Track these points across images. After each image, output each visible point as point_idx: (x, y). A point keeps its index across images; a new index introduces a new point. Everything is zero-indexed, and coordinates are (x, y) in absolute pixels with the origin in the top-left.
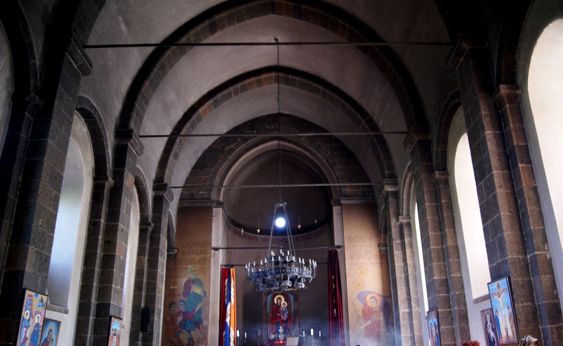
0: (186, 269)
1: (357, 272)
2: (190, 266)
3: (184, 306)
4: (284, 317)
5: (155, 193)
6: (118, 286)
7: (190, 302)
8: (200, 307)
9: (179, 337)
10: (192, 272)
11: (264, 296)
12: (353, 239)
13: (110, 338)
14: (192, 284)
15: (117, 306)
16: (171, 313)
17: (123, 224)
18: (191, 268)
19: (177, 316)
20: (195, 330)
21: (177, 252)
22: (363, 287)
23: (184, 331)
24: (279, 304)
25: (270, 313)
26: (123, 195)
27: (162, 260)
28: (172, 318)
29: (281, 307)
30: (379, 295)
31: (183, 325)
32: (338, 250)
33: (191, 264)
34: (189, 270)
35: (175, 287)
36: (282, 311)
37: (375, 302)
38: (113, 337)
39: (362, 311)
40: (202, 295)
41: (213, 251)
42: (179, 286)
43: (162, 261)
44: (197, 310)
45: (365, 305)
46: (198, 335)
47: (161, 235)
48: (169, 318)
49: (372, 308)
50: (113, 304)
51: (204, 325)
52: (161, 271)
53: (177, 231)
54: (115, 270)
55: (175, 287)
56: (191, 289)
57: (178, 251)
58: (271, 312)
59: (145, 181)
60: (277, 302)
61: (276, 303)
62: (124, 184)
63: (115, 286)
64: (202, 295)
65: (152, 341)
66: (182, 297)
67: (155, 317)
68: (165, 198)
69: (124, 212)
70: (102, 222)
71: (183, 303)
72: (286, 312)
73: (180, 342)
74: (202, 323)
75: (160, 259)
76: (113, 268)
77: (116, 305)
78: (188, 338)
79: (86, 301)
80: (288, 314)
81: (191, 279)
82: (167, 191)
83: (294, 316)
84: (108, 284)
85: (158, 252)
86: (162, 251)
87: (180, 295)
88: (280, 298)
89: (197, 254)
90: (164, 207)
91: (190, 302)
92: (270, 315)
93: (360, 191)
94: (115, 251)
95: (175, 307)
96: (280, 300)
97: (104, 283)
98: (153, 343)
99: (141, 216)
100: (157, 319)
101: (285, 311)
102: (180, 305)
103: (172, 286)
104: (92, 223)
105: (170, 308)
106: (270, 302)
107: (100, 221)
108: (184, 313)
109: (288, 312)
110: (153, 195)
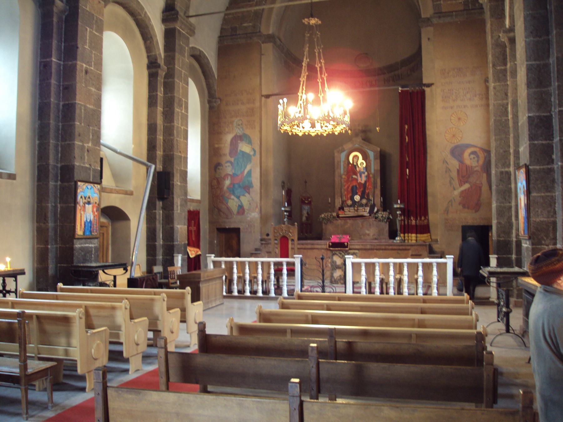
0: (232, 123)
1: (452, 118)
3: (231, 167)
4: (362, 180)
5: (165, 26)
6: (88, 143)
9: (227, 203)
10: (239, 127)
12: (448, 73)
13: (79, 207)
14: (239, 141)
15: (90, 169)
16: (217, 176)
17: (89, 63)
19: (224, 179)
20: (245, 196)
21: (219, 102)
22: (459, 139)
23: (233, 197)
24: (355, 164)
25: (344, 174)
26: (80, 23)
27: (183, 111)
28: (219, 183)
29: (358, 167)
30: (481, 149)
31: (232, 189)
32: (427, 90)
33: (237, 117)
34: (235, 124)
37: (476, 159)
38: (84, 207)
39: (456, 171)
40: (252, 153)
41: (263, 99)
43: (182, 113)
44: (246, 172)
45: (461, 162)
47: (176, 80)
48: (215, 182)
49: (471, 166)
50: (79, 166)
52: (182, 125)
53: (218, 76)
54: (77, 123)
56: (238, 147)
57: (220, 102)
58: (346, 173)
59: (142, 9)
61: (351, 162)
62: (80, 8)
63: (81, 144)
64: (252, 153)
65: (173, 210)
66: (228, 158)
67: (175, 180)
68: (179, 31)
69: (87, 47)
70: (54, 61)
72: (364, 173)
73: (228, 208)
75: (177, 110)
76: (74, 120)
77: (86, 167)
78: (237, 205)
79: (44, 164)
80: (366, 176)
82: (179, 22)
83: (374, 178)
84: (70, 141)
85: (174, 101)
86: (180, 100)
87: (226, 154)
88: (356, 156)
89: (243, 103)
90: (180, 45)
92: (344, 177)
93: (461, 2)
94: (75, 98)
95: (222, 169)
97: (66, 141)
98: (175, 212)
99: (148, 57)
100: (179, 184)
102: (226, 167)
103: (217, 144)
104: (43, 63)
105: (215, 170)
106: (344, 162)
107: (52, 61)
108: (233, 176)
109: (366, 173)
110: (164, 29)
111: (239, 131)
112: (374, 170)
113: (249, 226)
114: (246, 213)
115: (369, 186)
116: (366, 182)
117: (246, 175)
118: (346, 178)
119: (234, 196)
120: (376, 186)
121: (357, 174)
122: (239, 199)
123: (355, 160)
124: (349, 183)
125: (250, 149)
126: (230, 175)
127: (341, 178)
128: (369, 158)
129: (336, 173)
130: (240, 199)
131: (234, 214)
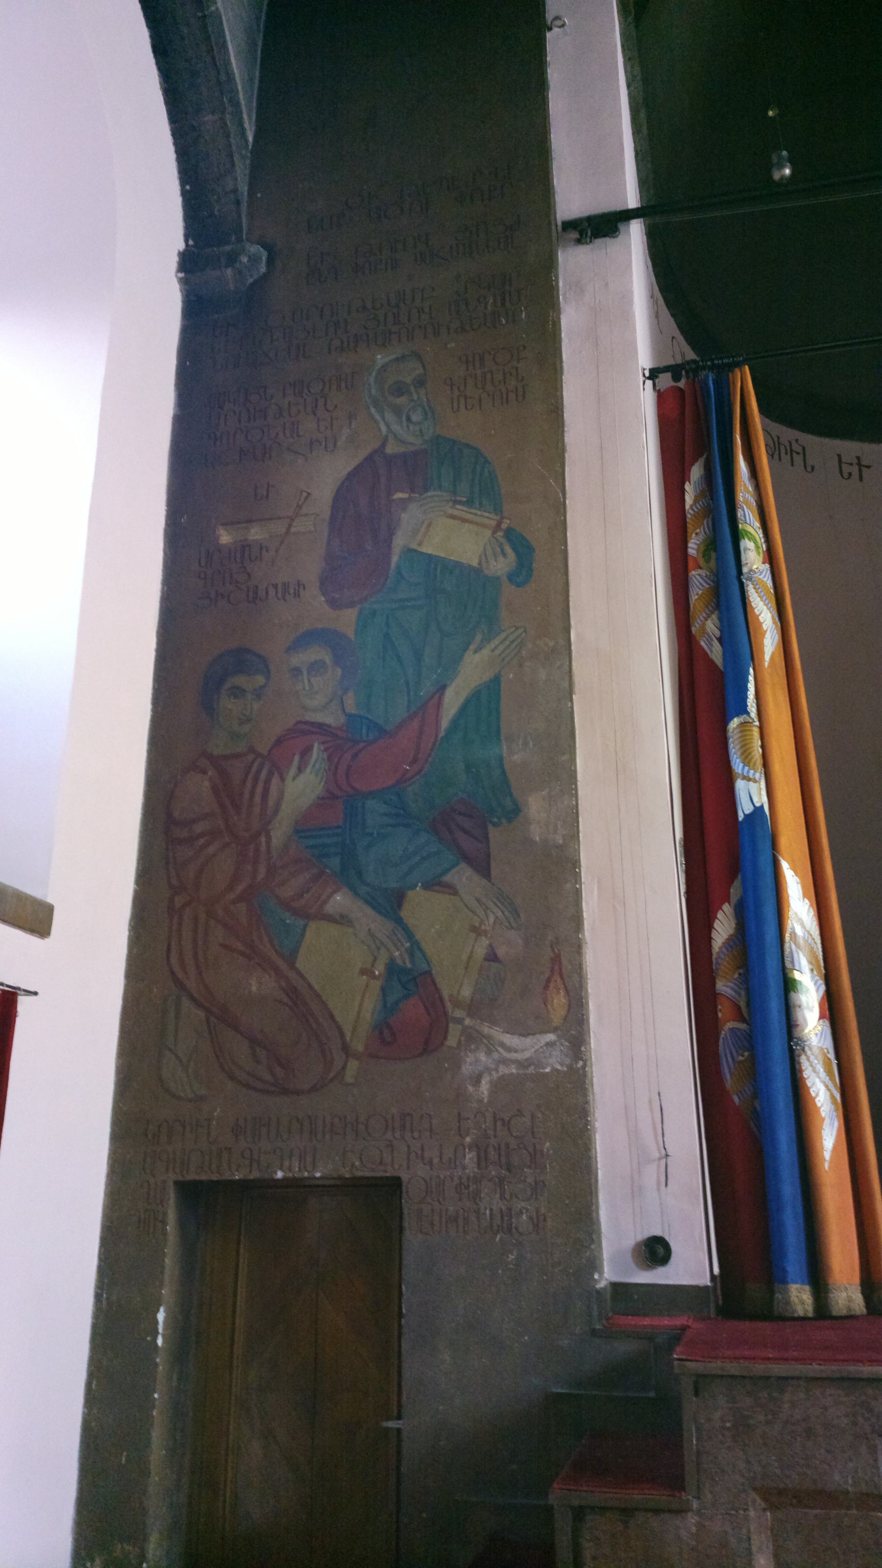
2: (380, 359)
7: (387, 636)
8: (488, 676)
9: (291, 959)
10: (402, 400)
14: (399, 495)
16: (219, 746)
18: (384, 367)
19: (278, 770)
20: (451, 889)
21: (263, 269)
35: (256, 533)
42: (292, 520)
46: (477, 931)
51: (536, 833)
55: (256, 533)
56: (391, 534)
57: (270, 261)
71: (325, 655)
74: (515, 812)
81: (390, 450)
91: (387, 636)
95: (258, 694)
102: (296, 672)
105: (208, 706)
111: (396, 428)
113: (482, 1160)
114: (454, 1031)
117: (455, 724)
119: (356, 893)
122: (399, 921)
125: (488, 533)
126: (322, 728)
130: (404, 913)
131: (345, 1048)
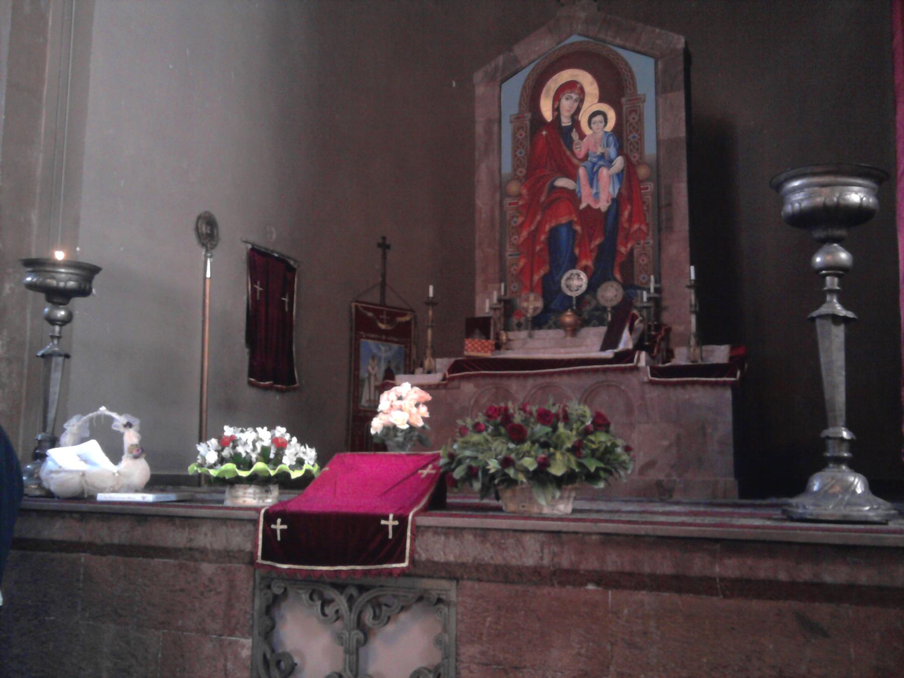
4: (597, 194)
11: (480, 90)
24: (566, 122)
25: (514, 177)
29: (582, 136)
36: (587, 156)
58: (522, 172)
60: (556, 110)
72: (610, 162)
80: (619, 175)
92: (514, 188)
96: (574, 96)
101: (602, 156)
106: (519, 117)
109: (619, 163)
112: (658, 142)
115: (630, 220)
116: (617, 203)
118: (524, 192)
120: (670, 219)
121: (576, 168)
123: (567, 105)
124: (538, 218)
127: (504, 194)
128: (634, 85)
129: (482, 174)
